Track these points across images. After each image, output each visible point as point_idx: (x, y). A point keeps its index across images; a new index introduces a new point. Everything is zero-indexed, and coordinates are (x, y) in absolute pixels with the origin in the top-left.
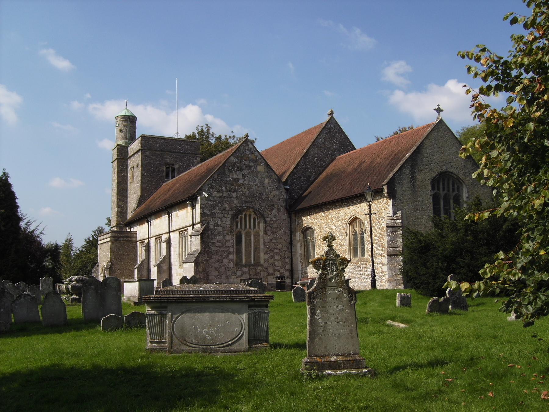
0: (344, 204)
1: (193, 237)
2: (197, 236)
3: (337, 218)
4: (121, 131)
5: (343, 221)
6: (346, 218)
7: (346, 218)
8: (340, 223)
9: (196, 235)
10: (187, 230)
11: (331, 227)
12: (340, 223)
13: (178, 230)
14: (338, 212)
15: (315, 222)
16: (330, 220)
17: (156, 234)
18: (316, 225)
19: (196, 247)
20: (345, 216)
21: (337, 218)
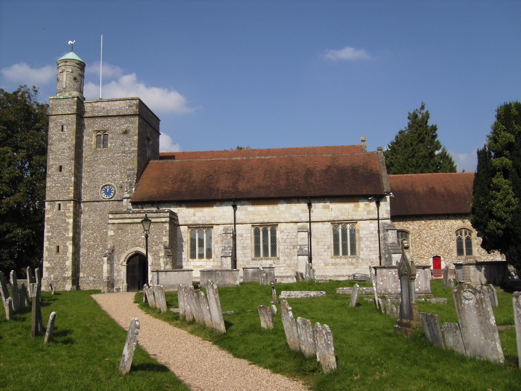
0: (450, 217)
1: (389, 231)
2: (393, 231)
3: (443, 226)
4: (75, 79)
5: (450, 230)
6: (452, 227)
7: (452, 227)
8: (445, 230)
9: (392, 230)
10: (356, 223)
11: (433, 232)
12: (445, 230)
13: (328, 221)
14: (443, 223)
15: (411, 227)
16: (432, 228)
17: (256, 222)
18: (413, 230)
19: (393, 240)
20: (452, 226)
21: (443, 226)
